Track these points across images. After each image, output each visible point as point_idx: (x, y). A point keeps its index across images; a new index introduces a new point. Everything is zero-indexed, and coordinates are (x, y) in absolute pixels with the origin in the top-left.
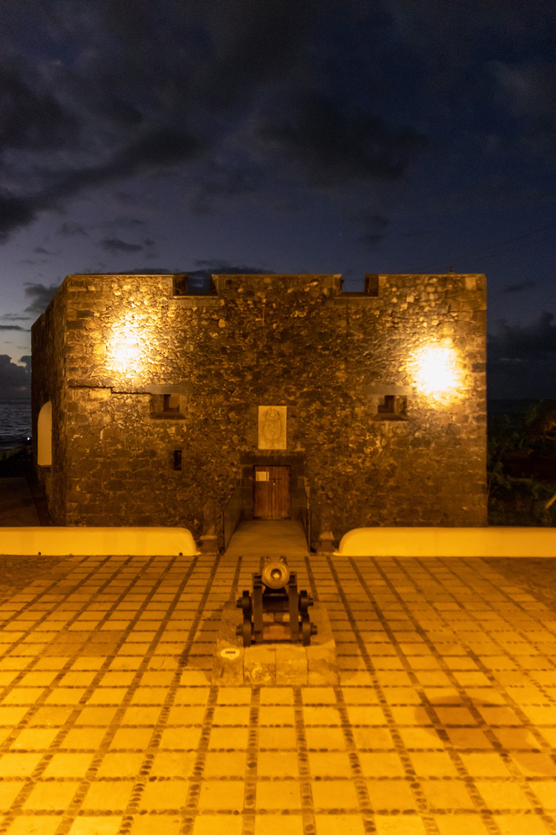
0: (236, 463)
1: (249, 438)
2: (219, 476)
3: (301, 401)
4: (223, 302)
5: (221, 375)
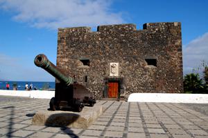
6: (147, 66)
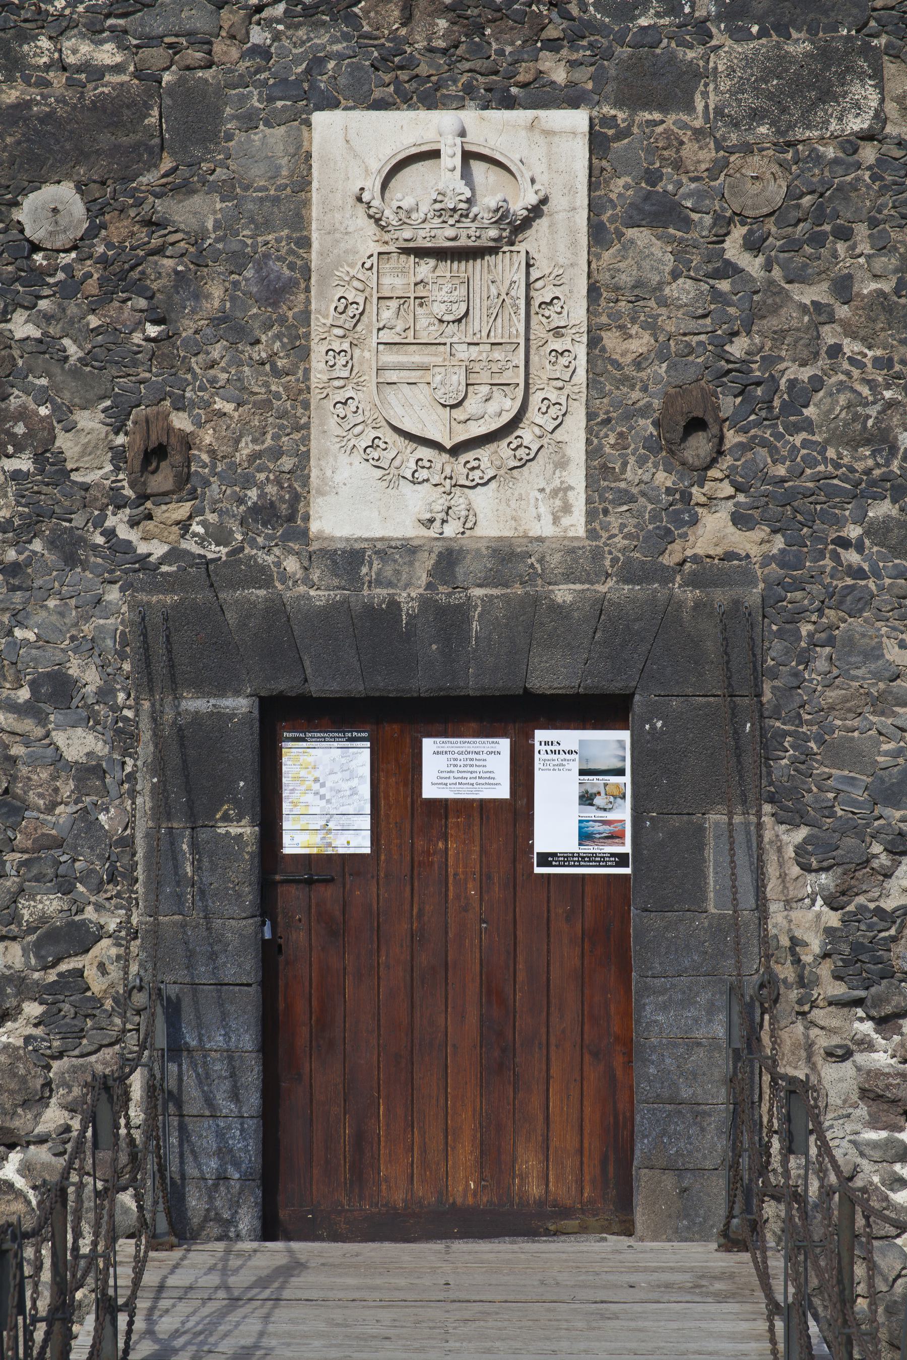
0: (91, 679)
1: (208, 427)
3: (728, 53)
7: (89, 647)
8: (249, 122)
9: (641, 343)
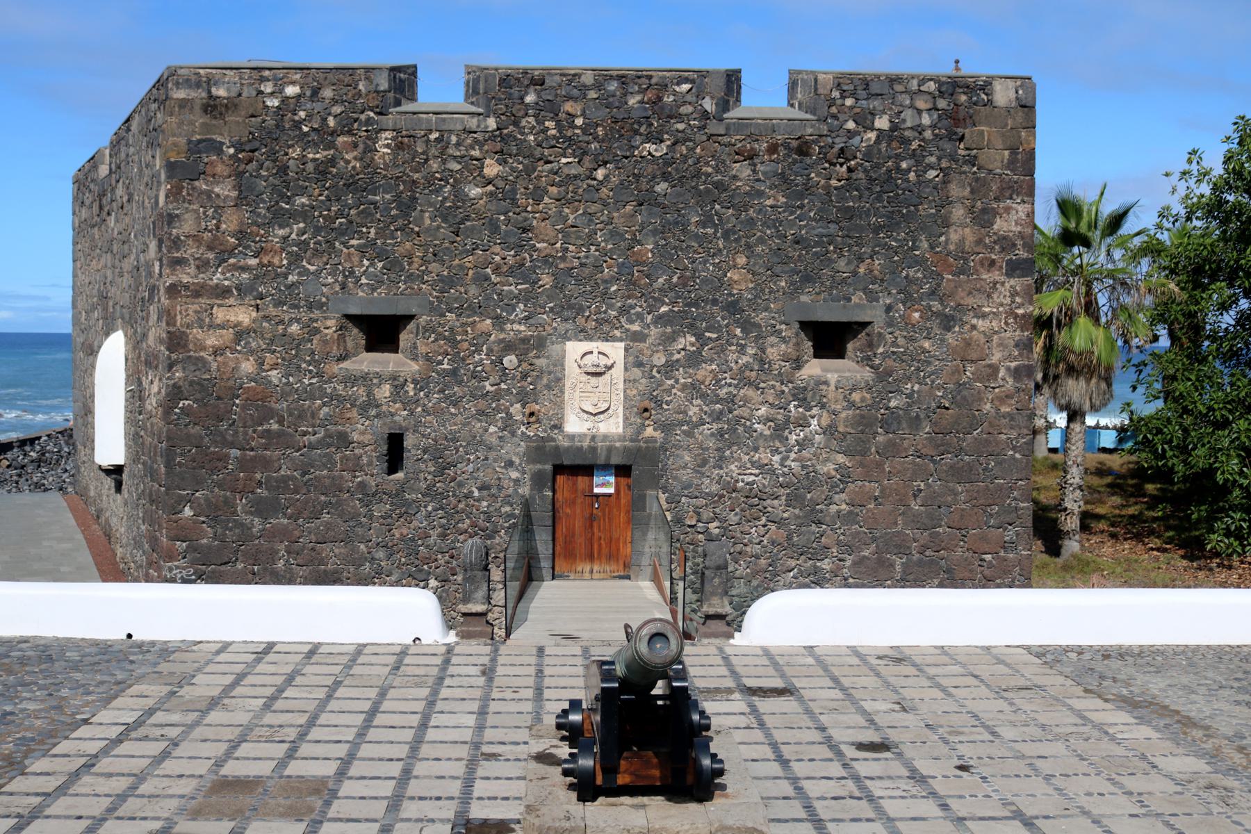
0: (517, 460)
2: (480, 489)
3: (654, 331)
4: (492, 123)
5: (487, 278)
6: (814, 368)
7: (517, 454)
8: (553, 343)
9: (635, 392)
